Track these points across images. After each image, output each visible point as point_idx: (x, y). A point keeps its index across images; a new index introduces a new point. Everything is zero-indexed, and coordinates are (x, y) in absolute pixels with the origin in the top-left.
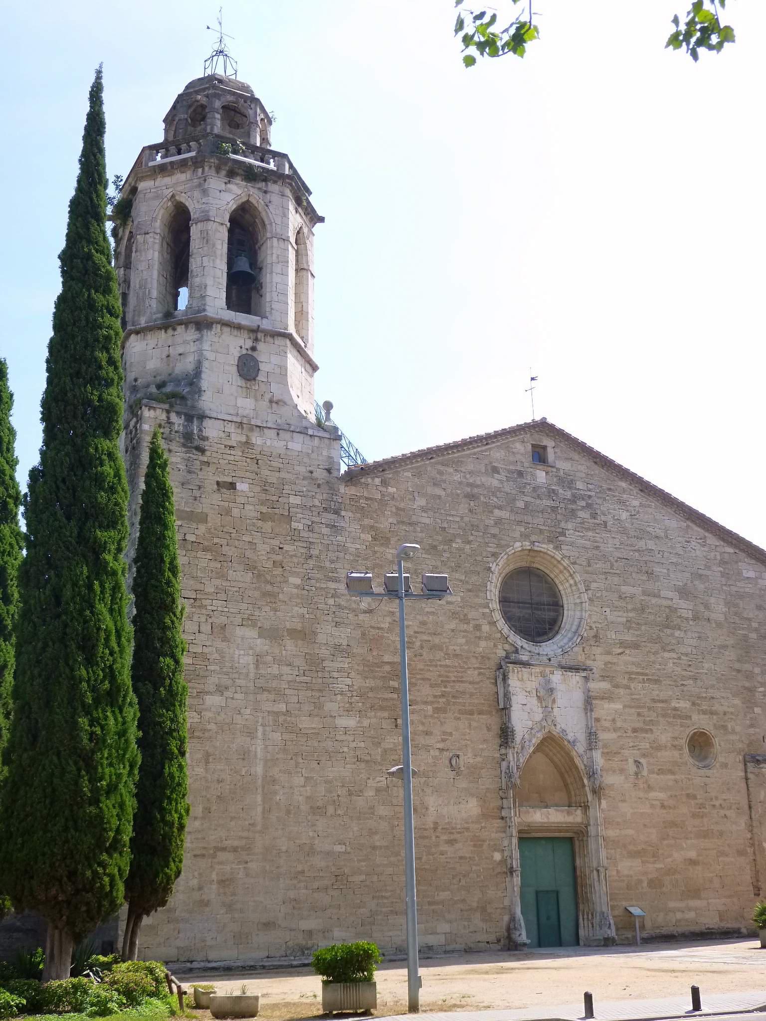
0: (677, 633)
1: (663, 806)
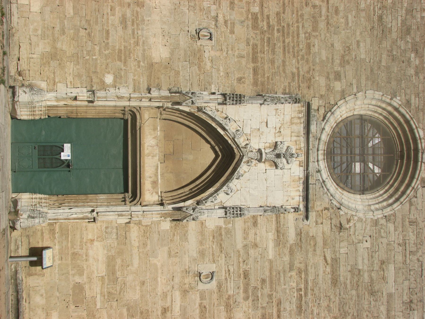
1: (165, 311)
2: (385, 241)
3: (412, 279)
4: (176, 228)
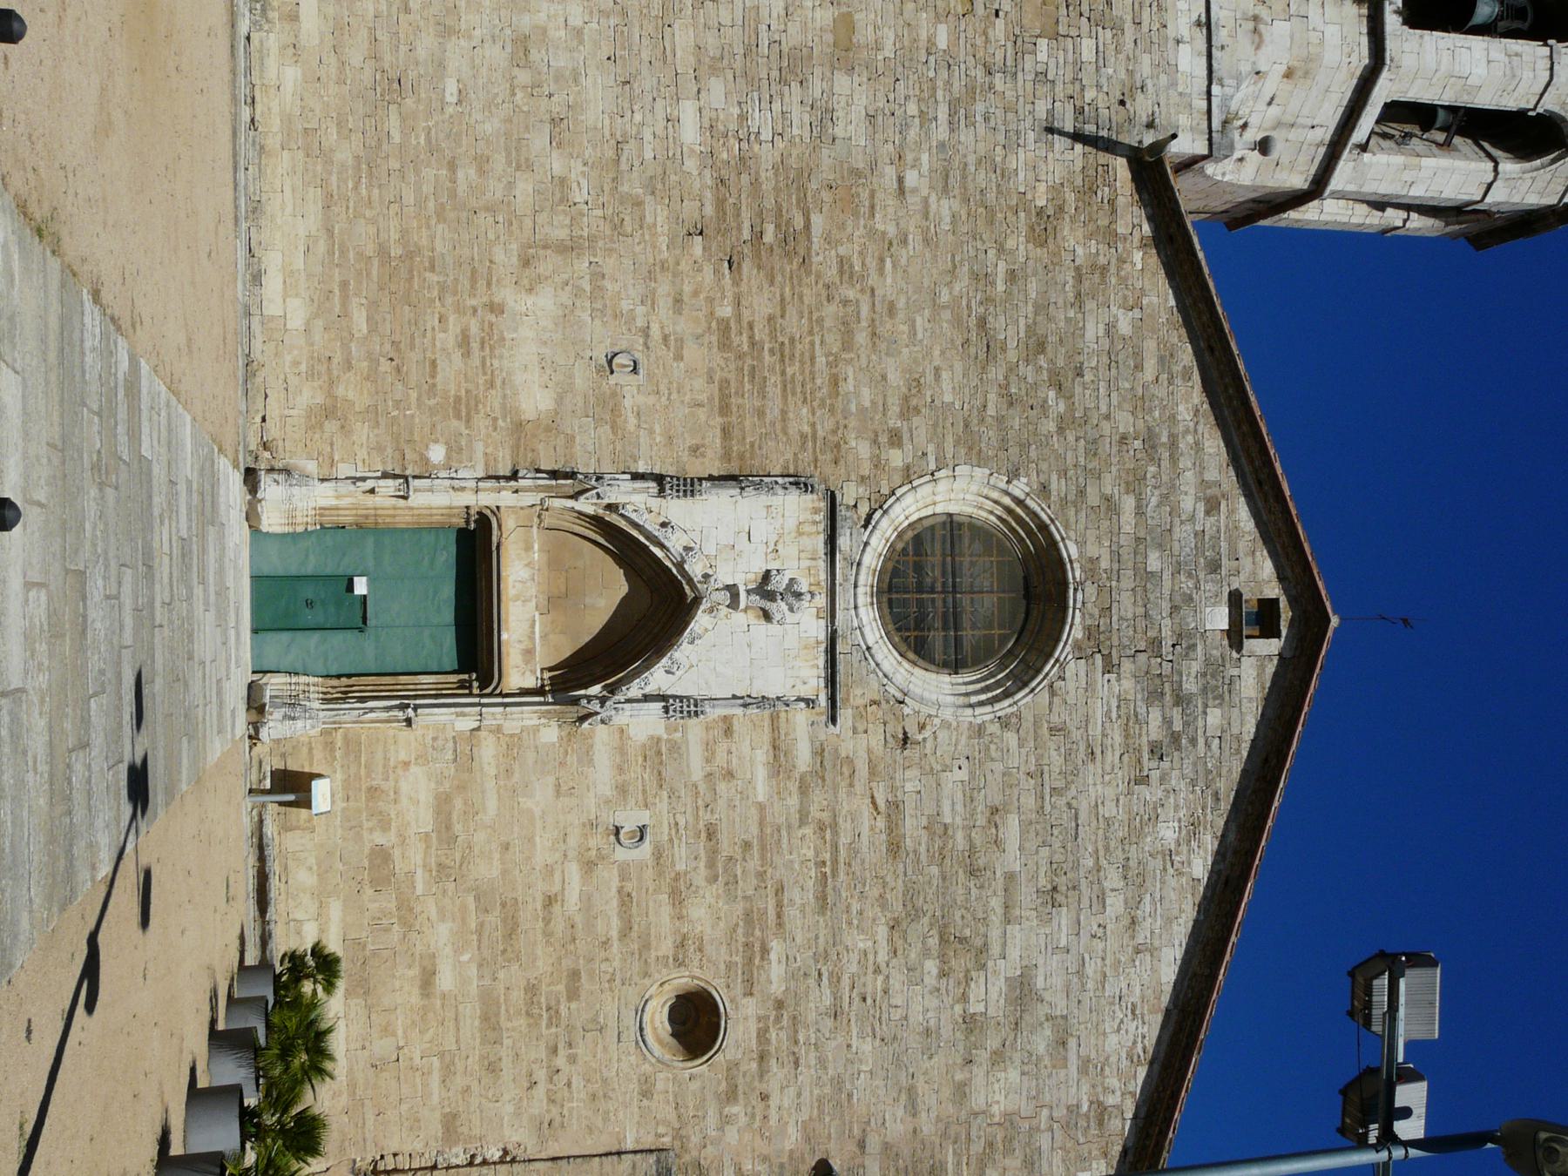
0: (931, 966)
1: (549, 901)
2: (999, 767)
3: (1057, 845)
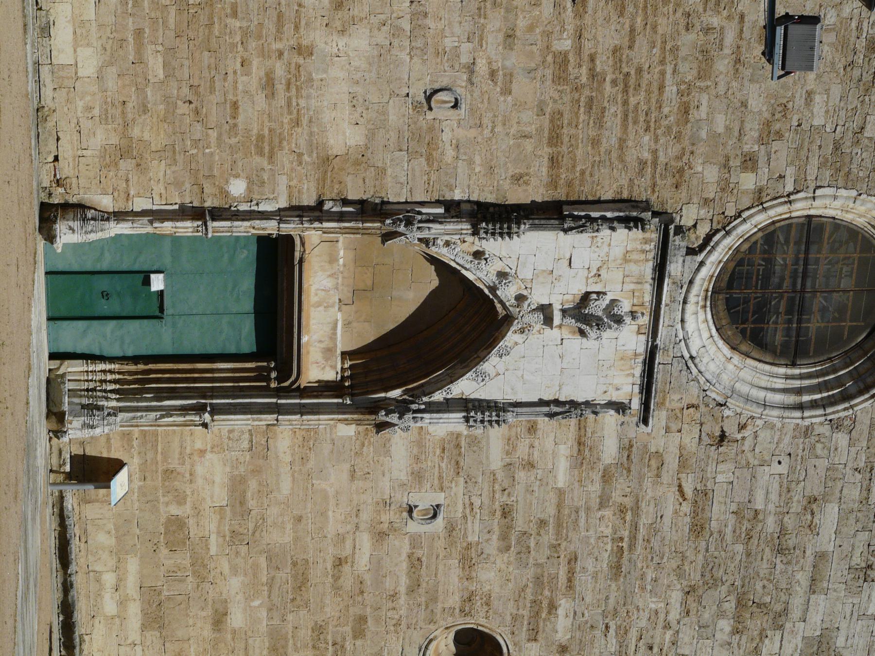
0: (725, 625)
1: (339, 562)
2: (823, 464)
4: (367, 435)
